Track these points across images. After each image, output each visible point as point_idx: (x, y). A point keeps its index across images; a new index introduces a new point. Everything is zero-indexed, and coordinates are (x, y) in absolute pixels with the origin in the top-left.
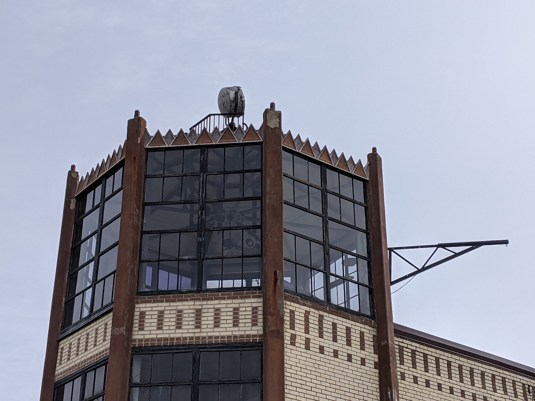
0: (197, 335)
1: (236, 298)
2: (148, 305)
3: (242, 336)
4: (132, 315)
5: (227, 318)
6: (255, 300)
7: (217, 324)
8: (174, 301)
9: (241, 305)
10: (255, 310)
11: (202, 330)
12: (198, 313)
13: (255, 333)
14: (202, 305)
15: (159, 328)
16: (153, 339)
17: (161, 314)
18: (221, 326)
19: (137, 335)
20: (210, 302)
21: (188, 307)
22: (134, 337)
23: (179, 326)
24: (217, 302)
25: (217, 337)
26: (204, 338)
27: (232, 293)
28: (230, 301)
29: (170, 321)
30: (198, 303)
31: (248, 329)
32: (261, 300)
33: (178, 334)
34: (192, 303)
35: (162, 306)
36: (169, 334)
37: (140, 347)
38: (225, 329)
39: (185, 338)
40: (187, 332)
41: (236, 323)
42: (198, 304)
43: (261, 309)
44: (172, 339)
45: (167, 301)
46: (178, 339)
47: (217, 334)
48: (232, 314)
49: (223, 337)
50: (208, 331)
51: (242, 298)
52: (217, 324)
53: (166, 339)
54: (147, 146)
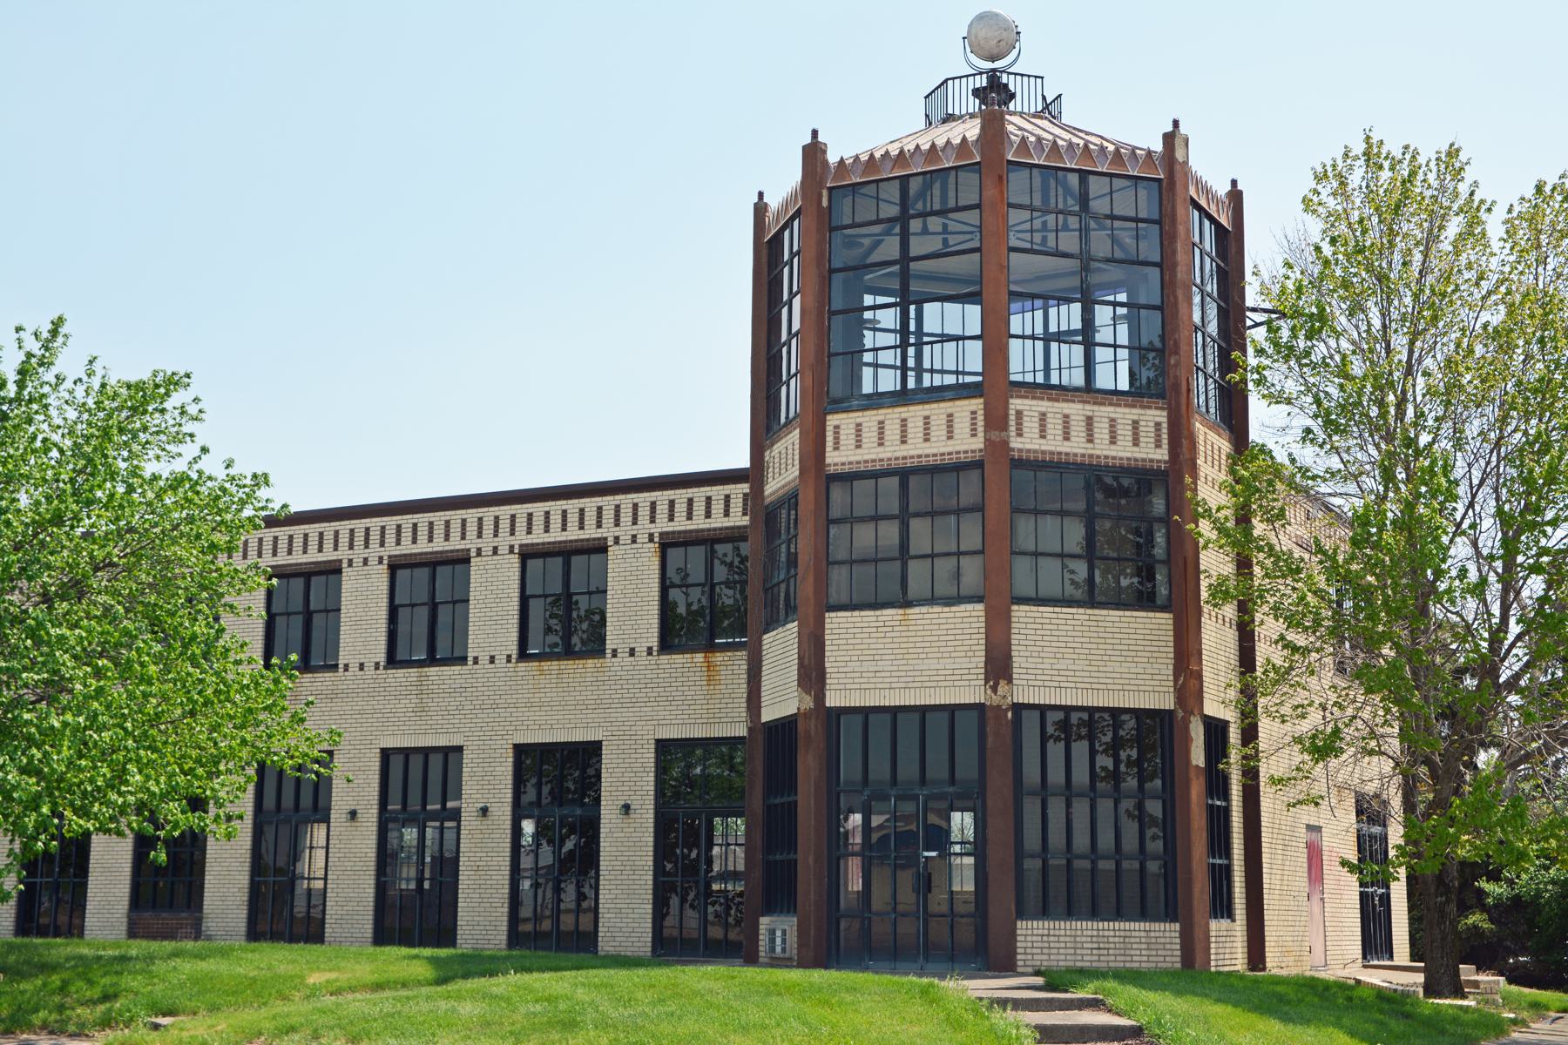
3: (1144, 460)
4: (1006, 415)
5: (1125, 432)
6: (1158, 412)
7: (1113, 440)
8: (1057, 400)
10: (1158, 424)
12: (1089, 421)
15: (1043, 437)
16: (1035, 451)
17: (1043, 417)
19: (1016, 443)
20: (1103, 408)
22: (1012, 445)
24: (1111, 409)
25: (1114, 458)
28: (1127, 410)
30: (1088, 407)
31: (1155, 453)
33: (1065, 447)
34: (1080, 406)
37: (1020, 460)
39: (1076, 455)
40: (1077, 446)
41: (1136, 442)
44: (1060, 453)
45: (1049, 399)
46: (1067, 454)
50: (1102, 449)
51: (1143, 407)
52: (1113, 440)
53: (1052, 453)
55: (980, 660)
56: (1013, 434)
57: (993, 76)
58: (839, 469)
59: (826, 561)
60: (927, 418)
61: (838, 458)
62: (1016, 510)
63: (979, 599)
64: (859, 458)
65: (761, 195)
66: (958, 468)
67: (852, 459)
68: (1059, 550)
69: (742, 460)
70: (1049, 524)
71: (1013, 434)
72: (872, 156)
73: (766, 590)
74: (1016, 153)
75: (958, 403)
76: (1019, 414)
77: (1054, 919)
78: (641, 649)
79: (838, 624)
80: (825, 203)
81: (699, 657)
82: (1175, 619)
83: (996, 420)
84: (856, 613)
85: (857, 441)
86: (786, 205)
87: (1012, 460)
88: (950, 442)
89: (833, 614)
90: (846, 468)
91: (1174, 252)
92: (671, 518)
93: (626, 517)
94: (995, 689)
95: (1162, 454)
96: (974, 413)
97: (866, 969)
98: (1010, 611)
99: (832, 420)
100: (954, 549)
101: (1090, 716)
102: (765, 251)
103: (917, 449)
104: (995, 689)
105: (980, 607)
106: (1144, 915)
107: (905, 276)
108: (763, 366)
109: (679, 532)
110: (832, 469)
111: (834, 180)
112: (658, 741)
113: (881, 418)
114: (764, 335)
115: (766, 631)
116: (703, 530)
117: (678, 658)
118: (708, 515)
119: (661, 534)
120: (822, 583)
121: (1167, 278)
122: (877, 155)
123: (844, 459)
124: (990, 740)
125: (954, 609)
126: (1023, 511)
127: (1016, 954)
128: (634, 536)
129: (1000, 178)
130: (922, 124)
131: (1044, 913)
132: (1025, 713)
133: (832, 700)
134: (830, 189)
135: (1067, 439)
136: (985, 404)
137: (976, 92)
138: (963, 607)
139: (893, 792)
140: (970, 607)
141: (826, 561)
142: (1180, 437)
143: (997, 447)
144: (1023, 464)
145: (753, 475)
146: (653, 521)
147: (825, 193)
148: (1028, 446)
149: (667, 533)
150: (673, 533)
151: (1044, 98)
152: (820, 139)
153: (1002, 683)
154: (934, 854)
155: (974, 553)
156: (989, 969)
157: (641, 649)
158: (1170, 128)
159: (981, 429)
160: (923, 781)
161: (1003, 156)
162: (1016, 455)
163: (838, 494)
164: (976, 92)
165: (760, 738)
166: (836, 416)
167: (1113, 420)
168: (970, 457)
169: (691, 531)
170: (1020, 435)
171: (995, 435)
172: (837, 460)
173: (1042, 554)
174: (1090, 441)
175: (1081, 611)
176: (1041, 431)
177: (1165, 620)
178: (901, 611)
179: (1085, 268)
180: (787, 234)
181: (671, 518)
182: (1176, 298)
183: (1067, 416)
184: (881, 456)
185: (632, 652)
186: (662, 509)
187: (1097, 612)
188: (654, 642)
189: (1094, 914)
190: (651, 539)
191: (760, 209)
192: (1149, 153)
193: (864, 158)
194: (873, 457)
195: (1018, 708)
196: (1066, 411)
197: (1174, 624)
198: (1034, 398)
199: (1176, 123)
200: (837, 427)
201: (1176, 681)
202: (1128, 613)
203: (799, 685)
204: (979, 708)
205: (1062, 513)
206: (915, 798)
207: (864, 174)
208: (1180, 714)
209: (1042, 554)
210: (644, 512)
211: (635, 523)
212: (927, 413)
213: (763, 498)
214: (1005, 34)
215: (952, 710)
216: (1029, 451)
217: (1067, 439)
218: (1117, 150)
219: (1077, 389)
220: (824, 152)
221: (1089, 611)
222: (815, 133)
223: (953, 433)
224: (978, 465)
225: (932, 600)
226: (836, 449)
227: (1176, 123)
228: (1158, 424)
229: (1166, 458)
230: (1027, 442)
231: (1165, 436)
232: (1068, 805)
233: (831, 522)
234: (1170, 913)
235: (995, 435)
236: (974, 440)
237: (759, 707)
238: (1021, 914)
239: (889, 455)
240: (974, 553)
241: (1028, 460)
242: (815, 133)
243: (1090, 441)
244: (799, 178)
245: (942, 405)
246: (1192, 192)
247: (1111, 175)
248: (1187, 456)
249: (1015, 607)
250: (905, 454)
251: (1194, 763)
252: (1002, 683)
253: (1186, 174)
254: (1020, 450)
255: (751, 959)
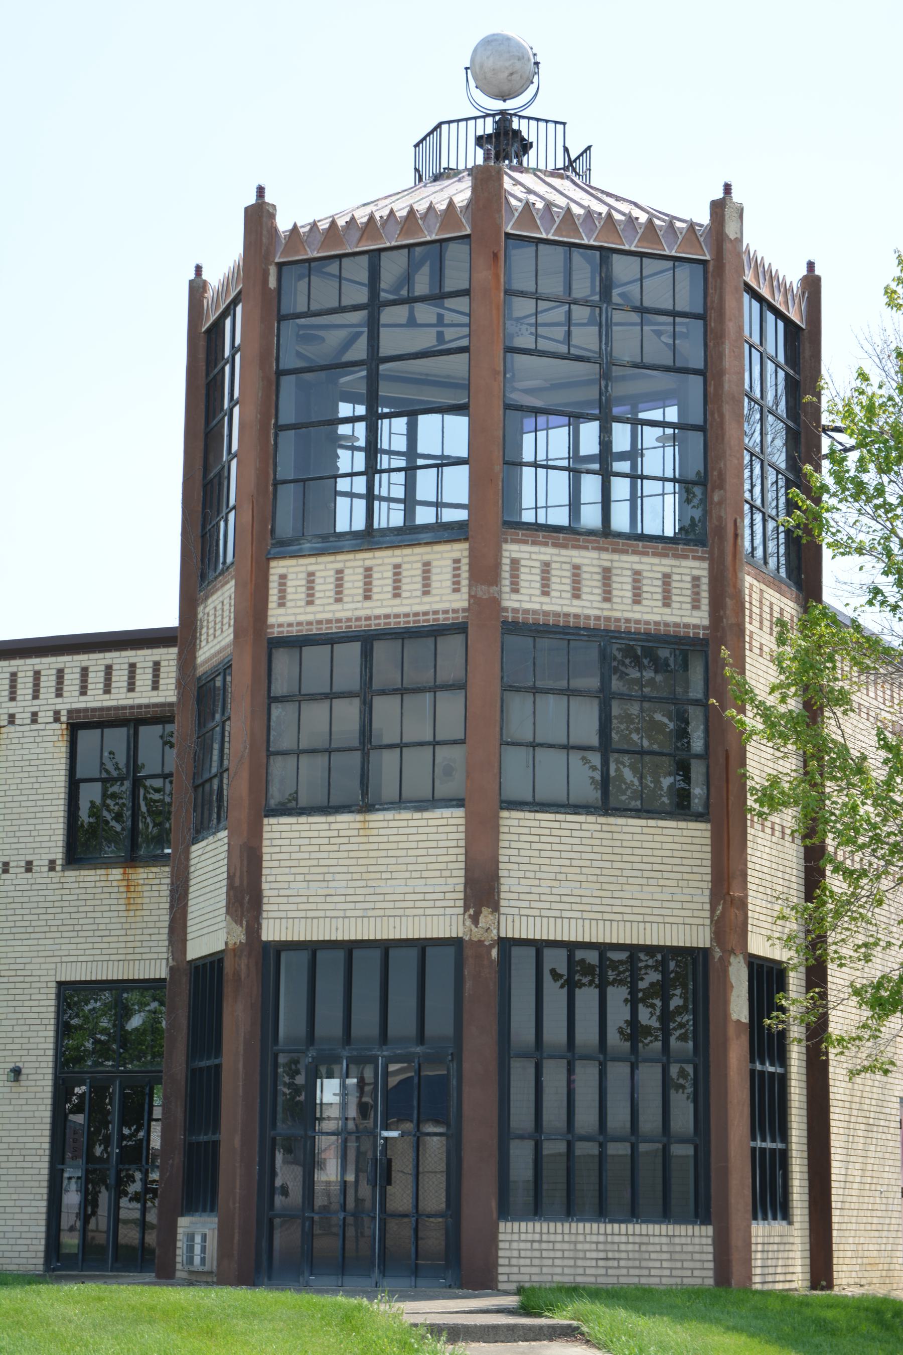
0: (606, 613)
1: (666, 556)
2: (525, 548)
3: (677, 625)
4: (498, 565)
5: (652, 589)
6: (696, 564)
7: (637, 599)
8: (565, 546)
9: (675, 570)
10: (696, 579)
11: (615, 606)
12: (607, 574)
13: (696, 621)
14: (612, 561)
15: (545, 593)
16: (535, 612)
17: (546, 567)
18: (645, 602)
19: (511, 601)
20: (625, 558)
21: (589, 559)
22: (506, 603)
23: (576, 594)
24: (635, 558)
25: (638, 622)
26: (618, 620)
27: (660, 545)
28: (656, 560)
29: (561, 582)
30: (605, 556)
31: (689, 615)
32: (705, 565)
33: (574, 608)
34: (594, 554)
35: (547, 553)
36: (562, 605)
37: (515, 623)
38: (649, 610)
39: (588, 617)
40: (589, 607)
41: (667, 602)
42: (606, 558)
43: (705, 580)
44: (567, 615)
45: (555, 545)
46: (577, 616)
47: (637, 616)
48: (659, 583)
49: (647, 623)
51: (676, 556)
52: (637, 599)
53: (557, 614)
54: (509, 230)
55: (458, 881)
56: (507, 589)
57: (504, 119)
58: (285, 631)
59: (266, 751)
60: (397, 566)
61: (286, 615)
62: (508, 688)
63: (459, 803)
64: (310, 617)
65: (198, 269)
66: (436, 632)
67: (301, 618)
68: (564, 741)
69: (168, 617)
70: (552, 706)
71: (507, 589)
72: (333, 223)
73: (196, 788)
74: (517, 224)
75: (438, 548)
76: (515, 563)
77: (548, 1220)
78: (41, 862)
79: (282, 836)
80: (272, 283)
81: (116, 874)
82: (713, 831)
83: (485, 571)
84: (303, 819)
85: (310, 594)
86: (227, 284)
87: (505, 623)
88: (426, 599)
89: (273, 820)
90: (294, 631)
91: (721, 356)
92: (83, 691)
93: (25, 688)
94: (475, 920)
95: (700, 618)
96: (457, 561)
97: (306, 1287)
98: (498, 818)
99: (277, 568)
100: (429, 738)
101: (602, 956)
102: (202, 343)
103: (385, 607)
104: (475, 920)
105: (460, 812)
106: (666, 1215)
107: (373, 380)
108: (198, 494)
109: (94, 710)
110: (275, 632)
111: (283, 253)
112: (60, 984)
113: (339, 566)
114: (200, 455)
115: (195, 841)
116: (124, 708)
117: (89, 876)
118: (131, 687)
119: (70, 712)
120: (261, 780)
121: (711, 389)
122: (341, 222)
123: (291, 619)
124: (468, 985)
125: (426, 815)
126: (518, 690)
127: (496, 1265)
128: (35, 714)
129: (495, 256)
130: (409, 179)
131: (537, 1210)
132: (516, 951)
133: (271, 931)
134: (280, 266)
135: (577, 596)
136: (471, 550)
137: (480, 141)
138: (438, 813)
139: (345, 1053)
140: (447, 812)
141: (266, 751)
142: (724, 597)
143: (485, 606)
144: (515, 628)
145: (181, 638)
146: (59, 694)
147: (273, 270)
148: (526, 606)
149: (78, 711)
150: (86, 710)
151: (566, 150)
152: (268, 199)
153: (485, 911)
154: (394, 1134)
155: (455, 742)
156: (461, 1287)
157: (41, 862)
158: (719, 195)
159: (465, 582)
160: (384, 1038)
161: (499, 228)
162: (510, 616)
163: (283, 661)
164: (480, 141)
165: (185, 980)
166: (283, 563)
167: (637, 573)
168: (451, 618)
169: (109, 709)
170: (515, 590)
171: (482, 591)
172: (281, 620)
173: (541, 745)
174: (607, 599)
175: (591, 819)
176: (543, 586)
177: (698, 833)
178: (359, 817)
179: (605, 376)
180: (228, 322)
181: (83, 691)
182: (722, 416)
183: (577, 567)
184: (339, 615)
185: (29, 867)
186: (72, 679)
187: (611, 820)
188: (58, 854)
189: (602, 1212)
190: (57, 720)
191: (197, 288)
192: (692, 226)
193: (324, 225)
194: (328, 616)
195: (506, 944)
196: (577, 561)
197: (713, 838)
198: (534, 543)
199: (727, 188)
200: (283, 577)
201: (713, 910)
202: (652, 823)
203: (228, 912)
204: (456, 943)
205: (569, 693)
206: (373, 1060)
207: (323, 245)
208: (717, 953)
209: (541, 745)
210: (48, 683)
211: (36, 697)
212: (397, 560)
213: (195, 668)
214: (518, 65)
215: (422, 946)
216: (526, 611)
217: (577, 596)
218: (650, 222)
219: (591, 533)
220: (272, 216)
221: (602, 820)
222: (261, 191)
223: (427, 587)
224: (461, 628)
225: (400, 803)
226: (282, 605)
227: (727, 188)
228: (696, 579)
229: (706, 622)
230: (525, 599)
231: (705, 594)
232: (570, 1071)
233: (272, 700)
234: (703, 1207)
235: (482, 591)
236: (456, 596)
237: (185, 941)
238: (505, 1212)
239: (348, 614)
240: (455, 742)
241: (525, 624)
242: (261, 191)
243: (607, 599)
244: (241, 250)
245: (418, 550)
246: (749, 277)
247: (642, 255)
248: (732, 620)
249: (504, 814)
250: (368, 612)
251: (734, 1017)
252: (485, 911)
253: (739, 255)
254: (516, 611)
255: (164, 1272)
